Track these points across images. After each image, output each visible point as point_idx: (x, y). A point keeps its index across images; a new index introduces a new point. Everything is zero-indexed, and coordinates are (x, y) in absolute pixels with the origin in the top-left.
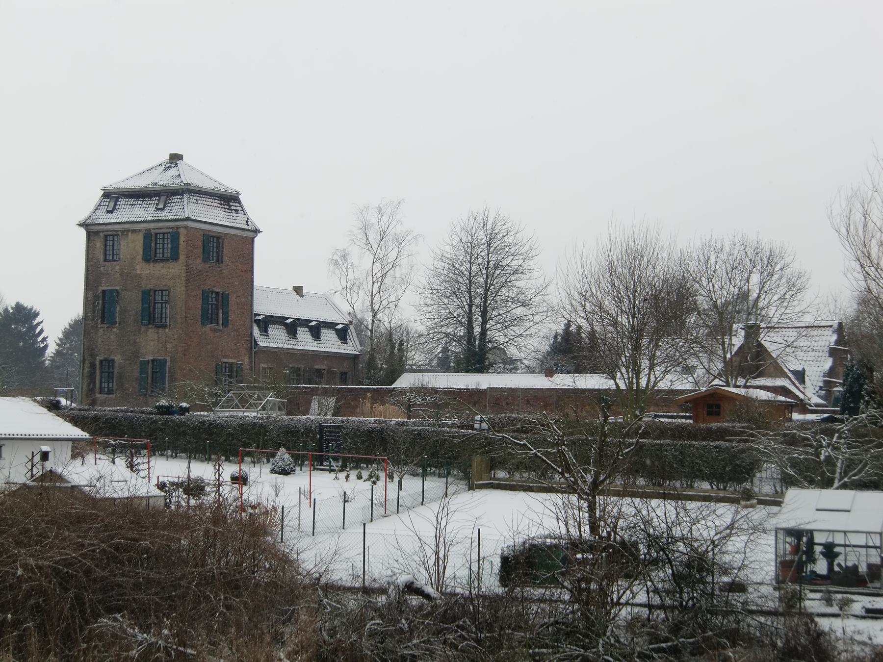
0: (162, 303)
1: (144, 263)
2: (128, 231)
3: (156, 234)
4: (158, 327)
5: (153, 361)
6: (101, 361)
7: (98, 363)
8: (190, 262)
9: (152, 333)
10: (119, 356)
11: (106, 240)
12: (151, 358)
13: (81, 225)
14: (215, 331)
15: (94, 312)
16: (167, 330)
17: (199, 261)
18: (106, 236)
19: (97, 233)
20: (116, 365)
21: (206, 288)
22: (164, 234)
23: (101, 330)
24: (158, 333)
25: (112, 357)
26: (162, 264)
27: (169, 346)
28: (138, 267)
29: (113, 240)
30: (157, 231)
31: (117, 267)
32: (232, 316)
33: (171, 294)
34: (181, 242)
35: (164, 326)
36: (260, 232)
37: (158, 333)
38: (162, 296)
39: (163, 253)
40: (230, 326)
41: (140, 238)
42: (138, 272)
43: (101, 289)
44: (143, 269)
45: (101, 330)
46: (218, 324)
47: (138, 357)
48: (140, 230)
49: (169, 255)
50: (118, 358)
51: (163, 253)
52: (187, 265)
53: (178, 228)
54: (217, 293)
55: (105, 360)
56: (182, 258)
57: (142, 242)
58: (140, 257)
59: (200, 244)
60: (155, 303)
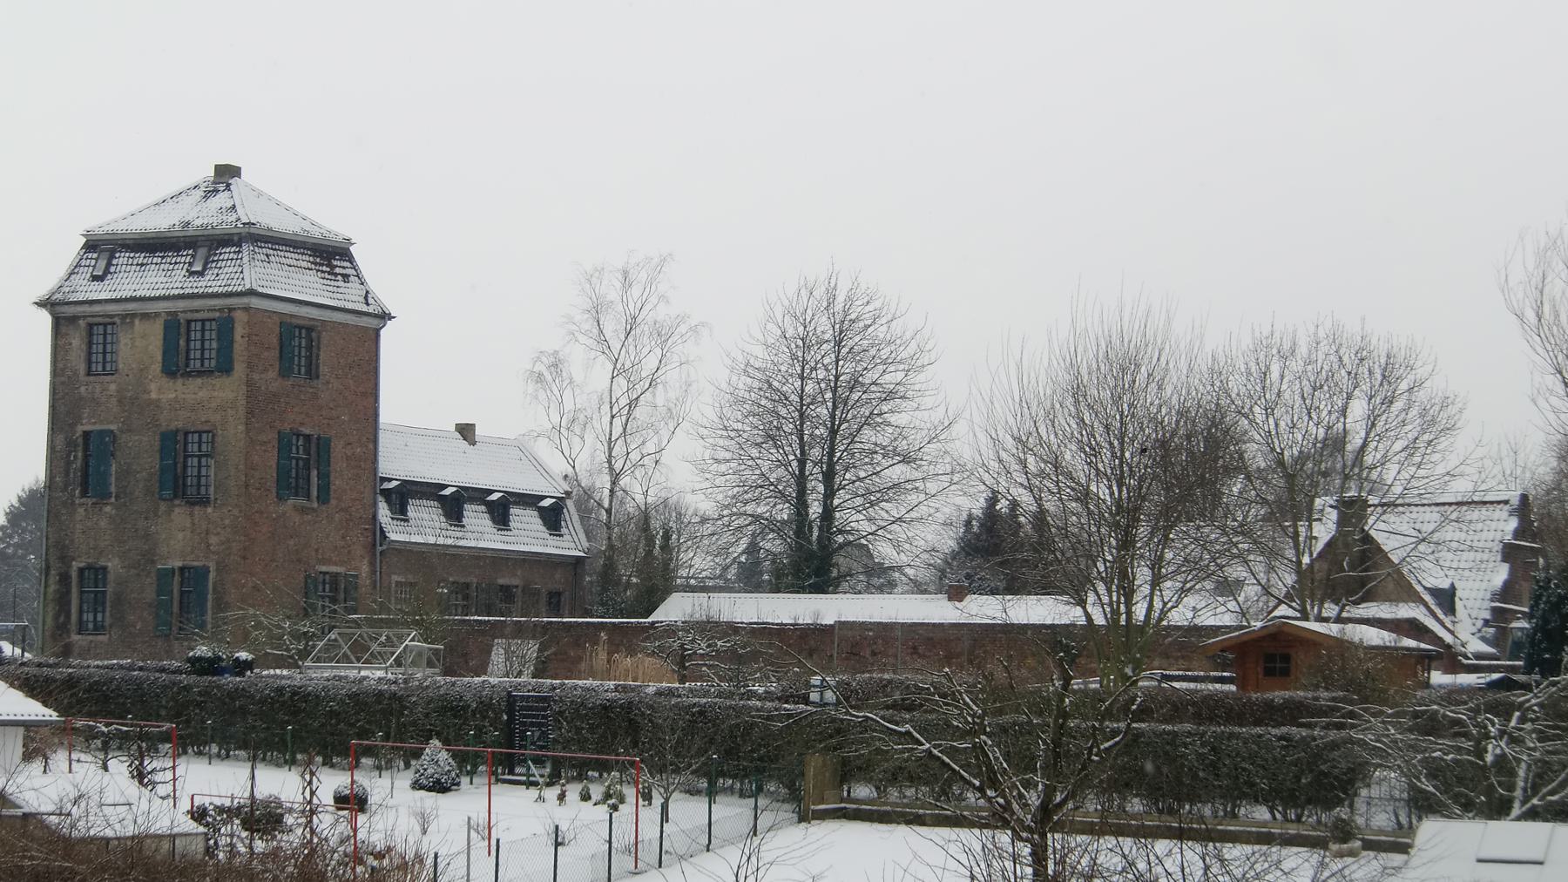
0: (200, 457)
1: (165, 380)
2: (133, 316)
3: (189, 322)
4: (193, 504)
5: (182, 569)
6: (81, 571)
7: (74, 574)
8: (256, 376)
9: (180, 515)
10: (116, 561)
11: (90, 335)
12: (180, 564)
13: (41, 304)
14: (303, 511)
15: (67, 474)
16: (210, 510)
17: (272, 374)
18: (91, 326)
19: (73, 319)
20: (111, 577)
21: (287, 427)
22: (203, 321)
23: (81, 510)
24: (192, 515)
25: (102, 563)
26: (199, 381)
27: (213, 540)
28: (153, 386)
29: (105, 334)
30: (190, 316)
31: (113, 387)
32: (337, 483)
33: (219, 439)
34: (237, 337)
35: (204, 502)
36: (391, 318)
37: (192, 515)
38: (200, 443)
39: (202, 359)
40: (333, 502)
41: (157, 329)
42: (154, 396)
43: (80, 429)
44: (163, 391)
45: (81, 510)
46: (308, 496)
47: (153, 562)
48: (157, 315)
49: (213, 363)
50: (113, 564)
51: (202, 359)
52: (249, 383)
53: (231, 310)
54: (308, 437)
55: (89, 567)
56: (239, 368)
57: (161, 337)
58: (157, 367)
59: (275, 341)
60: (186, 457)
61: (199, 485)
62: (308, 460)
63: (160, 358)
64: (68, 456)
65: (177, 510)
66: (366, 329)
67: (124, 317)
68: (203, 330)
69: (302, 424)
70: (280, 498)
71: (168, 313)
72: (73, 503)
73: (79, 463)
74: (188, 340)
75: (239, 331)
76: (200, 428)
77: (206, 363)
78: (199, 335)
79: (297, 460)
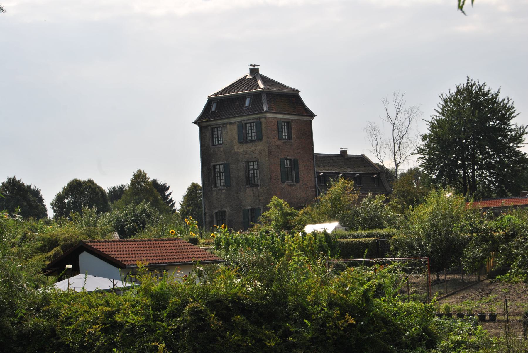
0: (220, 173)
1: (239, 145)
2: (227, 124)
3: (246, 124)
4: (253, 187)
5: (251, 209)
6: (216, 213)
7: (214, 215)
8: (271, 141)
9: (249, 191)
10: (228, 209)
11: (212, 131)
12: (250, 208)
13: (195, 123)
14: (291, 186)
15: (209, 180)
16: (259, 188)
17: (276, 139)
18: (212, 129)
19: (206, 127)
20: (227, 214)
21: (283, 157)
22: (251, 123)
23: (215, 192)
24: (253, 190)
25: (224, 209)
26: (251, 144)
27: (261, 198)
28: (235, 147)
29: (217, 131)
30: (246, 122)
31: (222, 149)
32: (302, 175)
33: (260, 163)
34: (263, 128)
35: (257, 186)
36: (315, 116)
37: (253, 190)
38: (220, 168)
39: (252, 136)
40: (301, 182)
41: (235, 127)
42: (236, 151)
43: (212, 164)
44: (238, 149)
45: (215, 192)
46: (293, 181)
47: (241, 208)
48: (235, 123)
49: (255, 137)
50: (227, 210)
51: (252, 136)
52: (268, 143)
53: (260, 118)
54: (290, 160)
55: (219, 212)
56: (265, 138)
57: (236, 130)
58: (236, 141)
59: (276, 127)
60: (249, 171)
61: (254, 180)
62: (291, 168)
63: (237, 138)
64: (209, 174)
65: (247, 189)
66: (307, 121)
67: (223, 124)
68: (251, 126)
69: (288, 156)
70: (283, 182)
71: (239, 122)
72: (212, 190)
73: (212, 176)
74: (246, 130)
75: (263, 125)
76: (253, 160)
77: (253, 138)
78: (250, 128)
79: (287, 168)
